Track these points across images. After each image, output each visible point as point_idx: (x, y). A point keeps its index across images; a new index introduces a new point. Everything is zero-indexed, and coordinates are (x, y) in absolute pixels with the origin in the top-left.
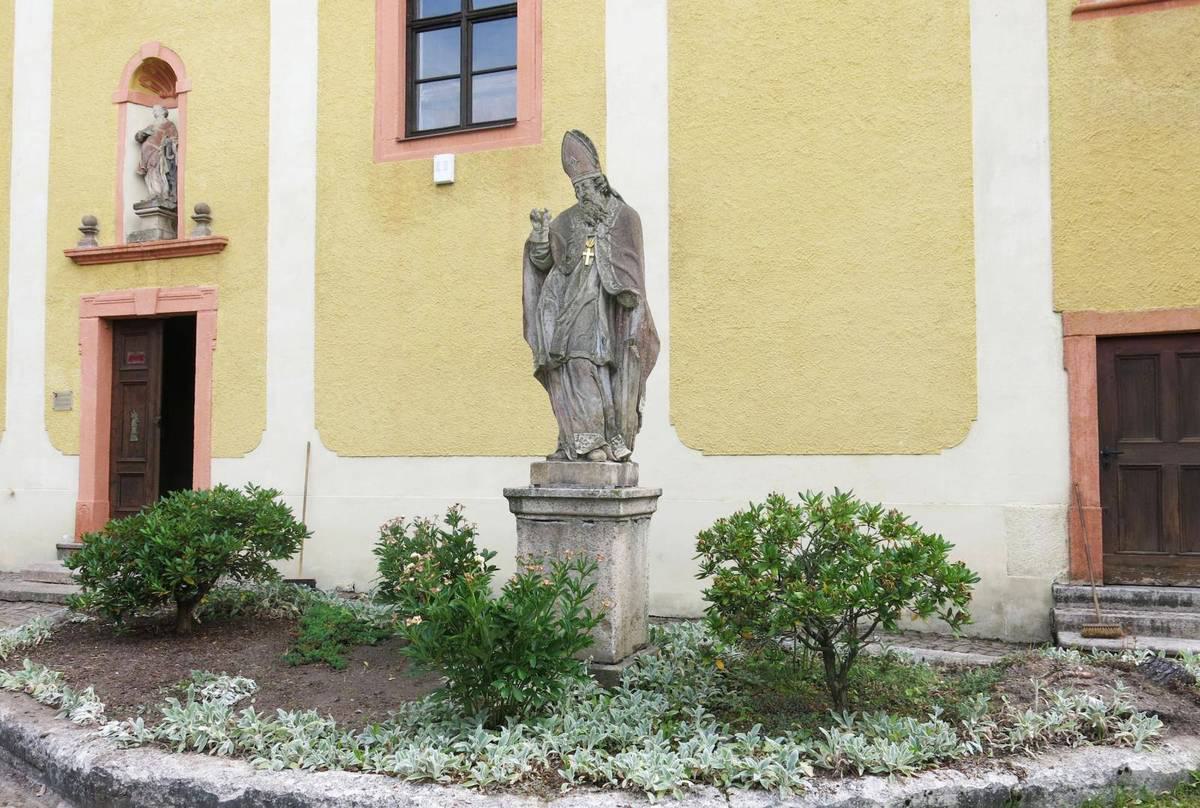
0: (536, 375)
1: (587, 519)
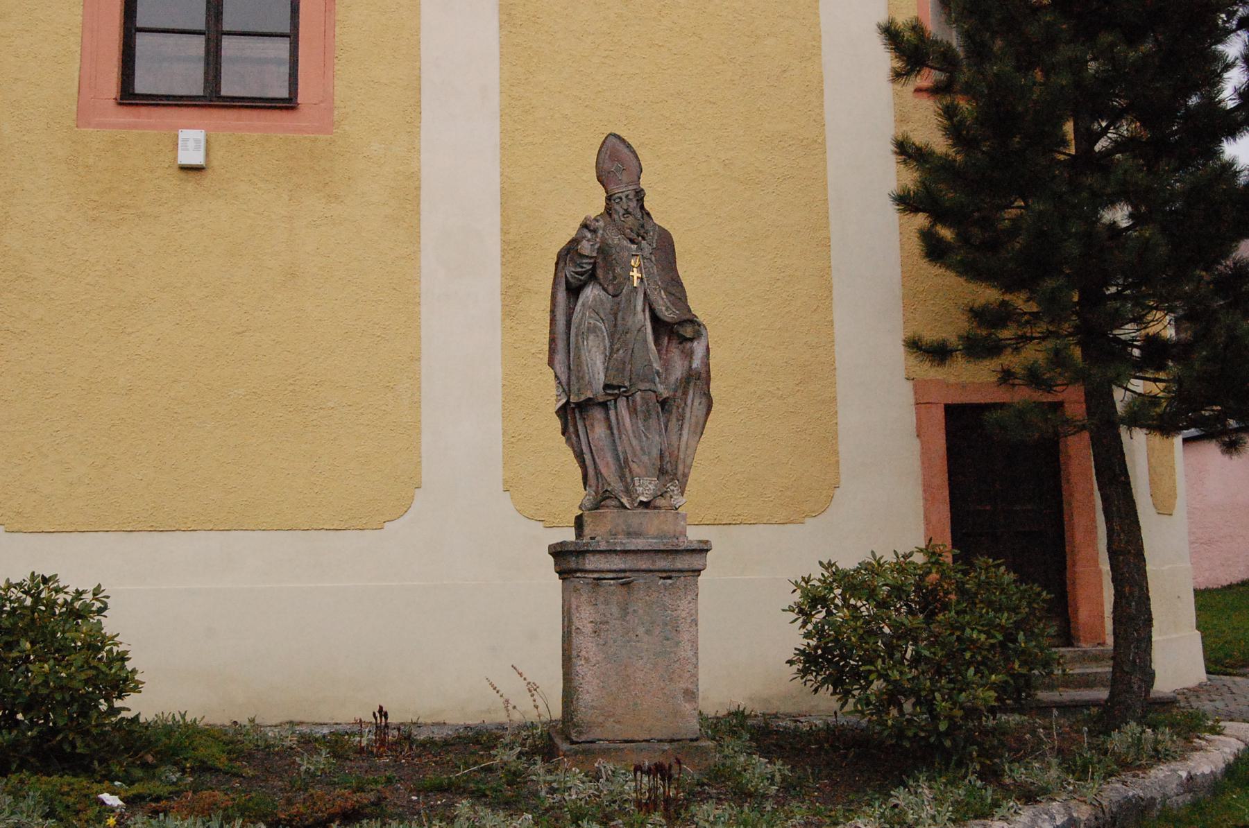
0: (556, 412)
1: (664, 575)
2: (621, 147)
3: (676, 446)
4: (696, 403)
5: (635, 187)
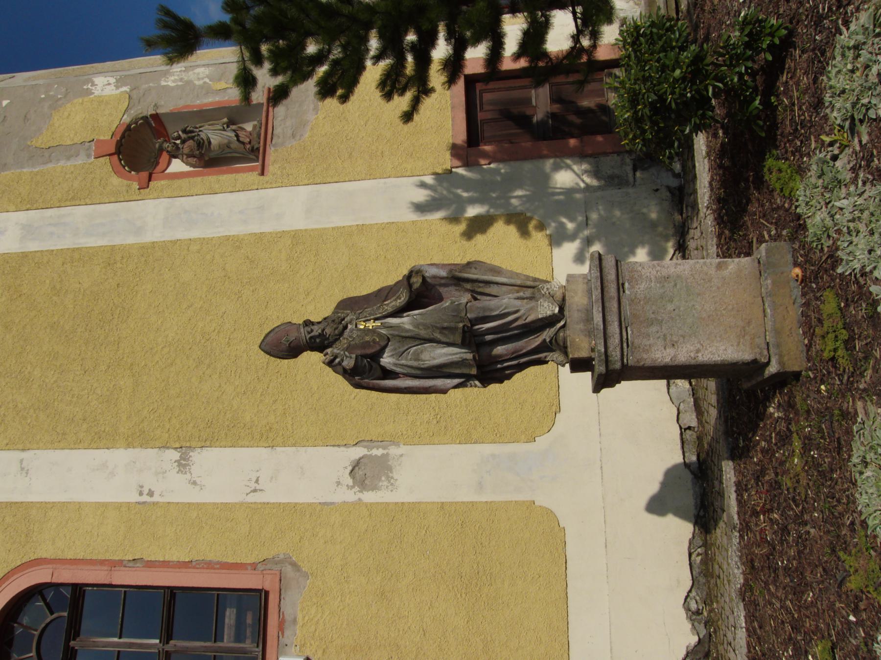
0: (485, 387)
1: (621, 290)
2: (269, 338)
3: (511, 288)
5: (302, 327)
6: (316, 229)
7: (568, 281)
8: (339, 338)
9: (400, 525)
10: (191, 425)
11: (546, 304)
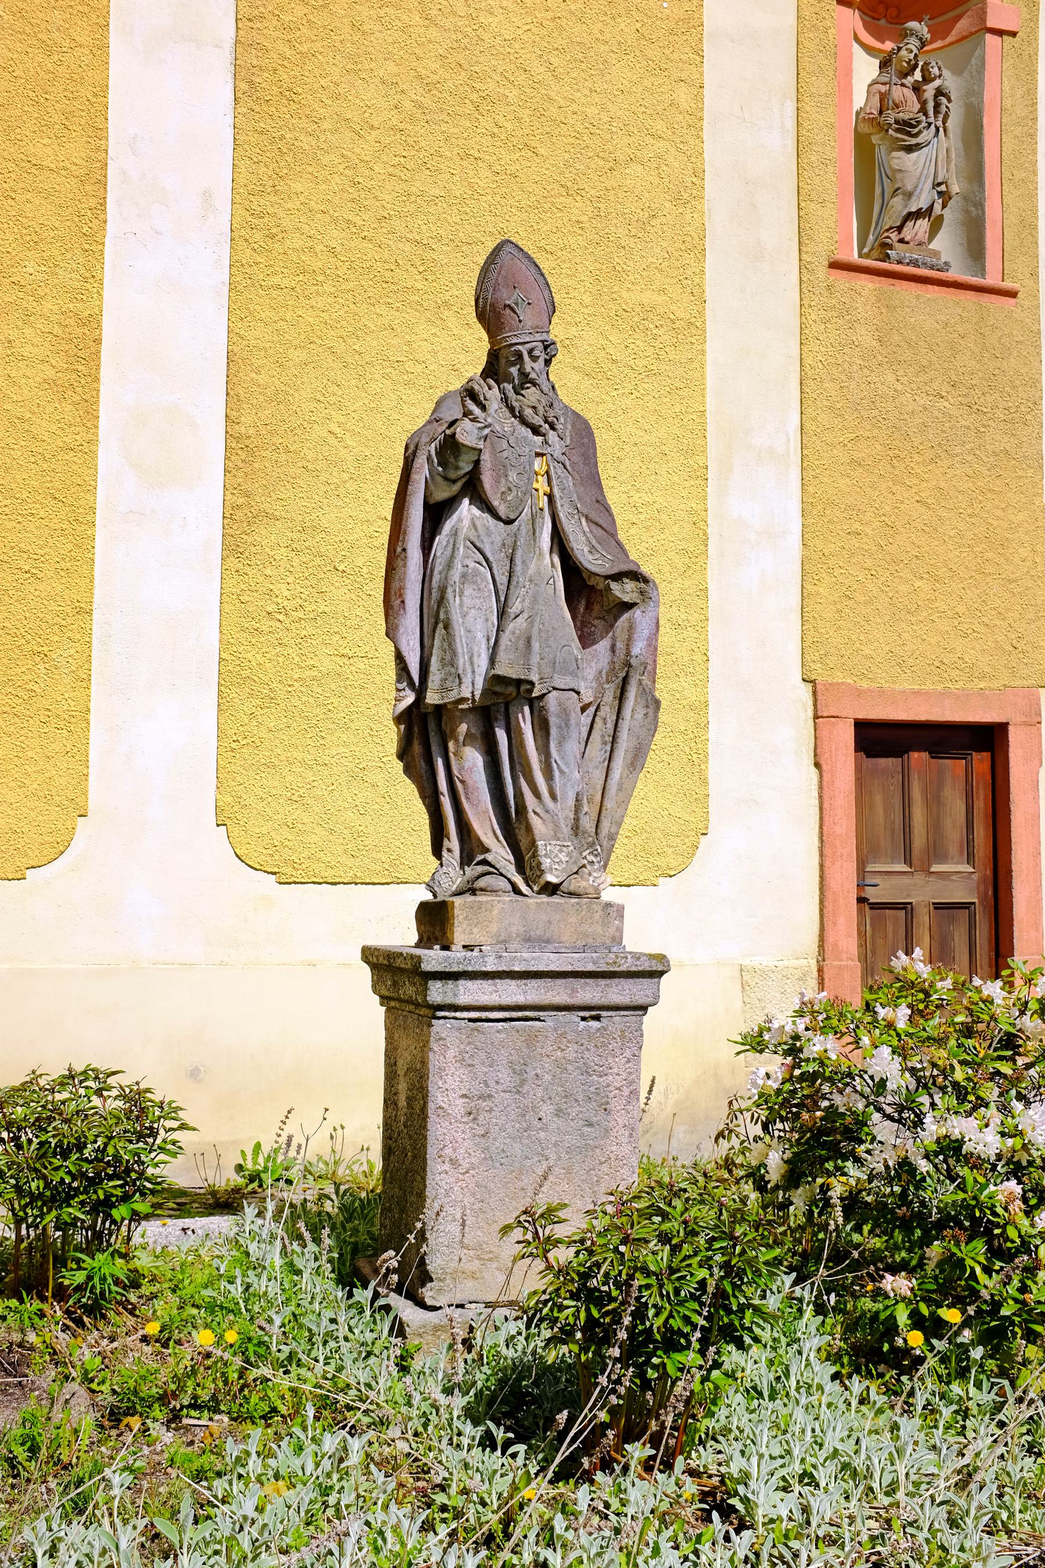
1: (586, 1014)
4: (639, 716)
6: (703, 377)
7: (609, 905)
8: (515, 417)
9: (42, 514)
10: (288, 53)
11: (563, 857)
